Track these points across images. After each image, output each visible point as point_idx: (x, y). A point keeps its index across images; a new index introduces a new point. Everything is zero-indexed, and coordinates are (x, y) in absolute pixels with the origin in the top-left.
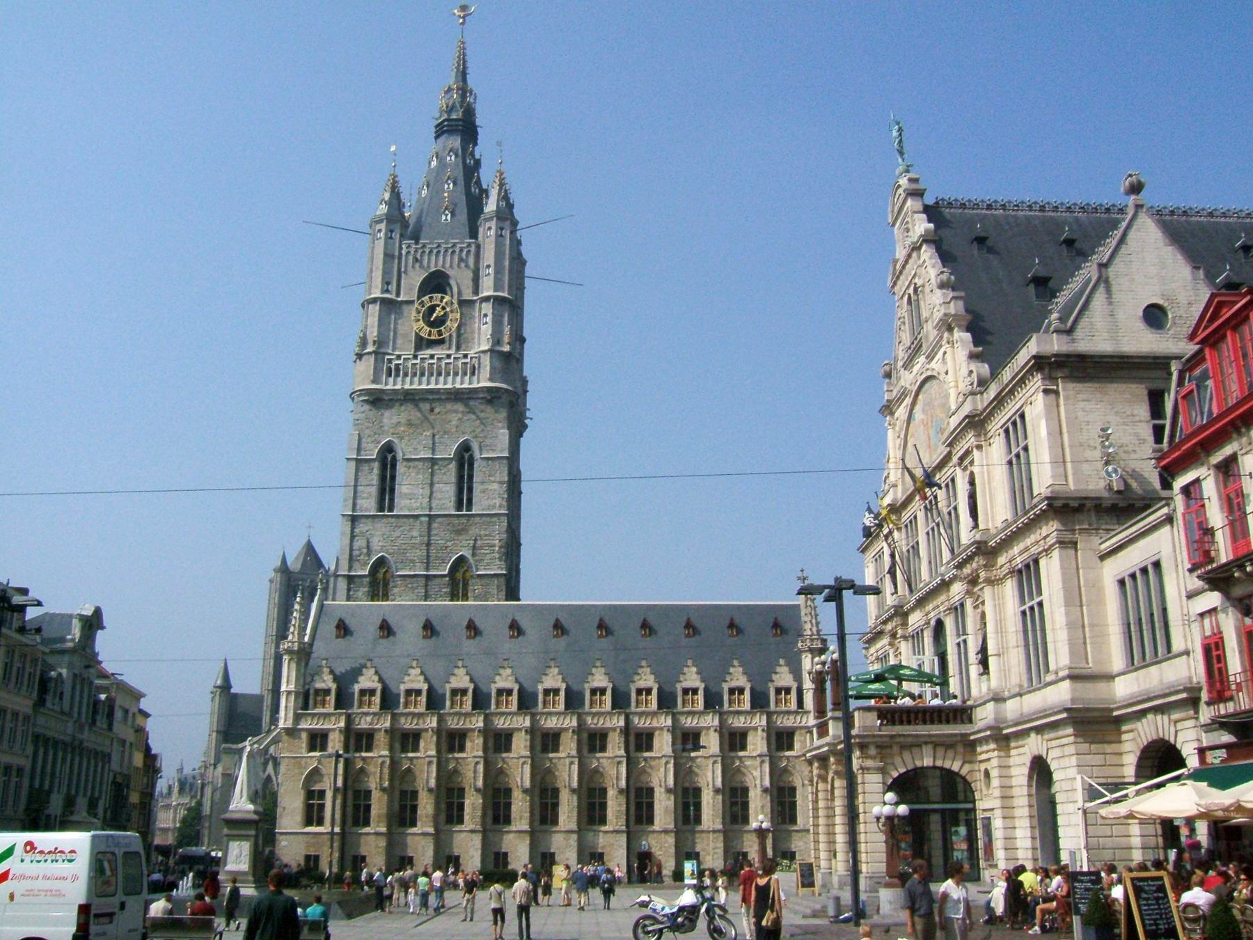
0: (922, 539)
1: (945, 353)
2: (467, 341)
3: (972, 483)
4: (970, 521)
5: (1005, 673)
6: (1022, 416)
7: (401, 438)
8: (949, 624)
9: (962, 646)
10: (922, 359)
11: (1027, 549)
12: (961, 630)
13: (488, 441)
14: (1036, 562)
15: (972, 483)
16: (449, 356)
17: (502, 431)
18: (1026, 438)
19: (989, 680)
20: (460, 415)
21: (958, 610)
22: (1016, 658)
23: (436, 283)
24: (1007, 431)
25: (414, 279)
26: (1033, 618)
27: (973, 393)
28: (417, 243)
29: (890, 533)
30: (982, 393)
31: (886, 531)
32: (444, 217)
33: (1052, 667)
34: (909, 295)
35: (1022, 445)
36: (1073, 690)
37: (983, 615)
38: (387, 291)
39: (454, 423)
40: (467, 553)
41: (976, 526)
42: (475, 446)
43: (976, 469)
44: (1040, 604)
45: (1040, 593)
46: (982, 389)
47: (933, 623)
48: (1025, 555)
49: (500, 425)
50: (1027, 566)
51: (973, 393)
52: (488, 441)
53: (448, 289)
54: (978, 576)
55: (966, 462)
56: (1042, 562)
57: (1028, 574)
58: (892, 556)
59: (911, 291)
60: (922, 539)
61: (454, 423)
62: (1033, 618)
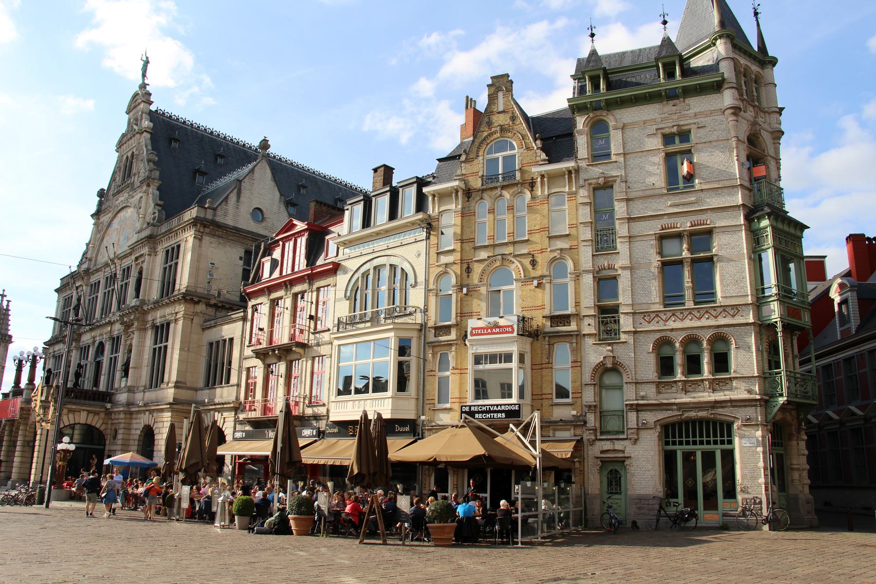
1: (141, 197)
3: (140, 273)
4: (134, 293)
8: (108, 347)
9: (113, 361)
10: (126, 195)
11: (164, 316)
14: (168, 324)
15: (140, 273)
19: (127, 381)
21: (116, 341)
22: (145, 373)
24: (167, 251)
27: (153, 225)
30: (159, 226)
33: (166, 379)
34: (127, 157)
35: (174, 262)
37: (131, 345)
41: (137, 296)
43: (145, 266)
44: (166, 347)
45: (167, 341)
46: (159, 224)
48: (163, 319)
50: (162, 325)
51: (153, 225)
54: (133, 324)
56: (172, 326)
57: (162, 331)
59: (129, 154)
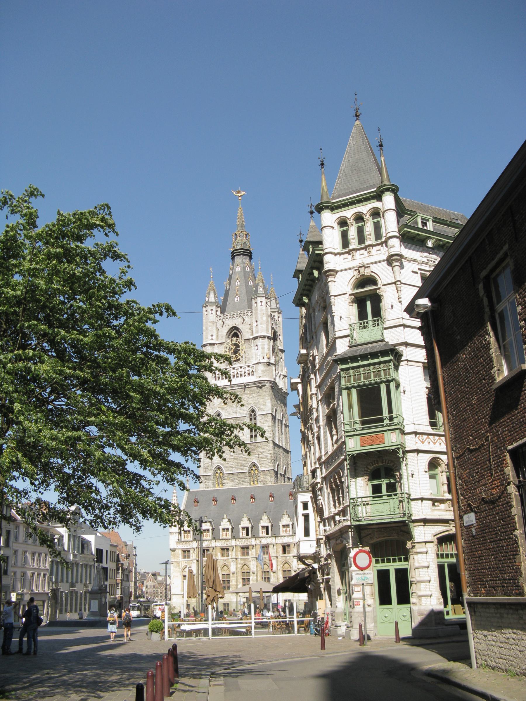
2: (249, 359)
7: (223, 409)
13: (262, 407)
16: (241, 367)
17: (267, 401)
20: (248, 395)
23: (235, 332)
25: (225, 331)
28: (224, 315)
32: (236, 299)
38: (212, 339)
39: (246, 399)
40: (256, 461)
42: (256, 409)
49: (267, 398)
52: (262, 407)
53: (239, 334)
61: (246, 399)
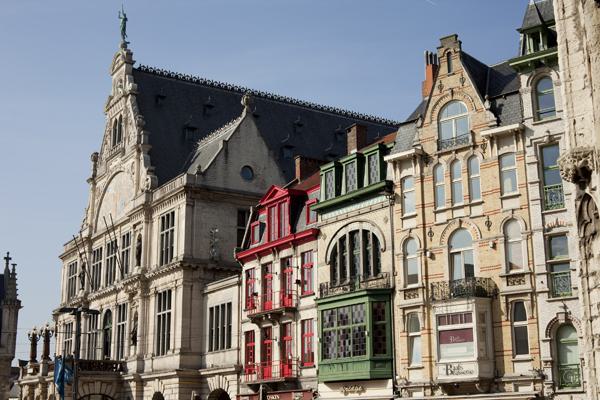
0: (103, 262)
3: (140, 240)
4: (135, 261)
5: (144, 347)
6: (173, 213)
9: (121, 329)
11: (166, 284)
12: (122, 317)
15: (140, 240)
18: (173, 225)
19: (135, 349)
22: (151, 339)
24: (163, 218)
26: (164, 322)
29: (85, 252)
31: (82, 251)
33: (172, 347)
36: (181, 360)
37: (136, 313)
41: (139, 264)
43: (143, 233)
44: (169, 314)
45: (170, 308)
47: (104, 311)
48: (164, 286)
50: (165, 293)
55: (138, 227)
56: (173, 293)
57: (164, 298)
58: (84, 267)
60: (103, 262)
62: (164, 322)
